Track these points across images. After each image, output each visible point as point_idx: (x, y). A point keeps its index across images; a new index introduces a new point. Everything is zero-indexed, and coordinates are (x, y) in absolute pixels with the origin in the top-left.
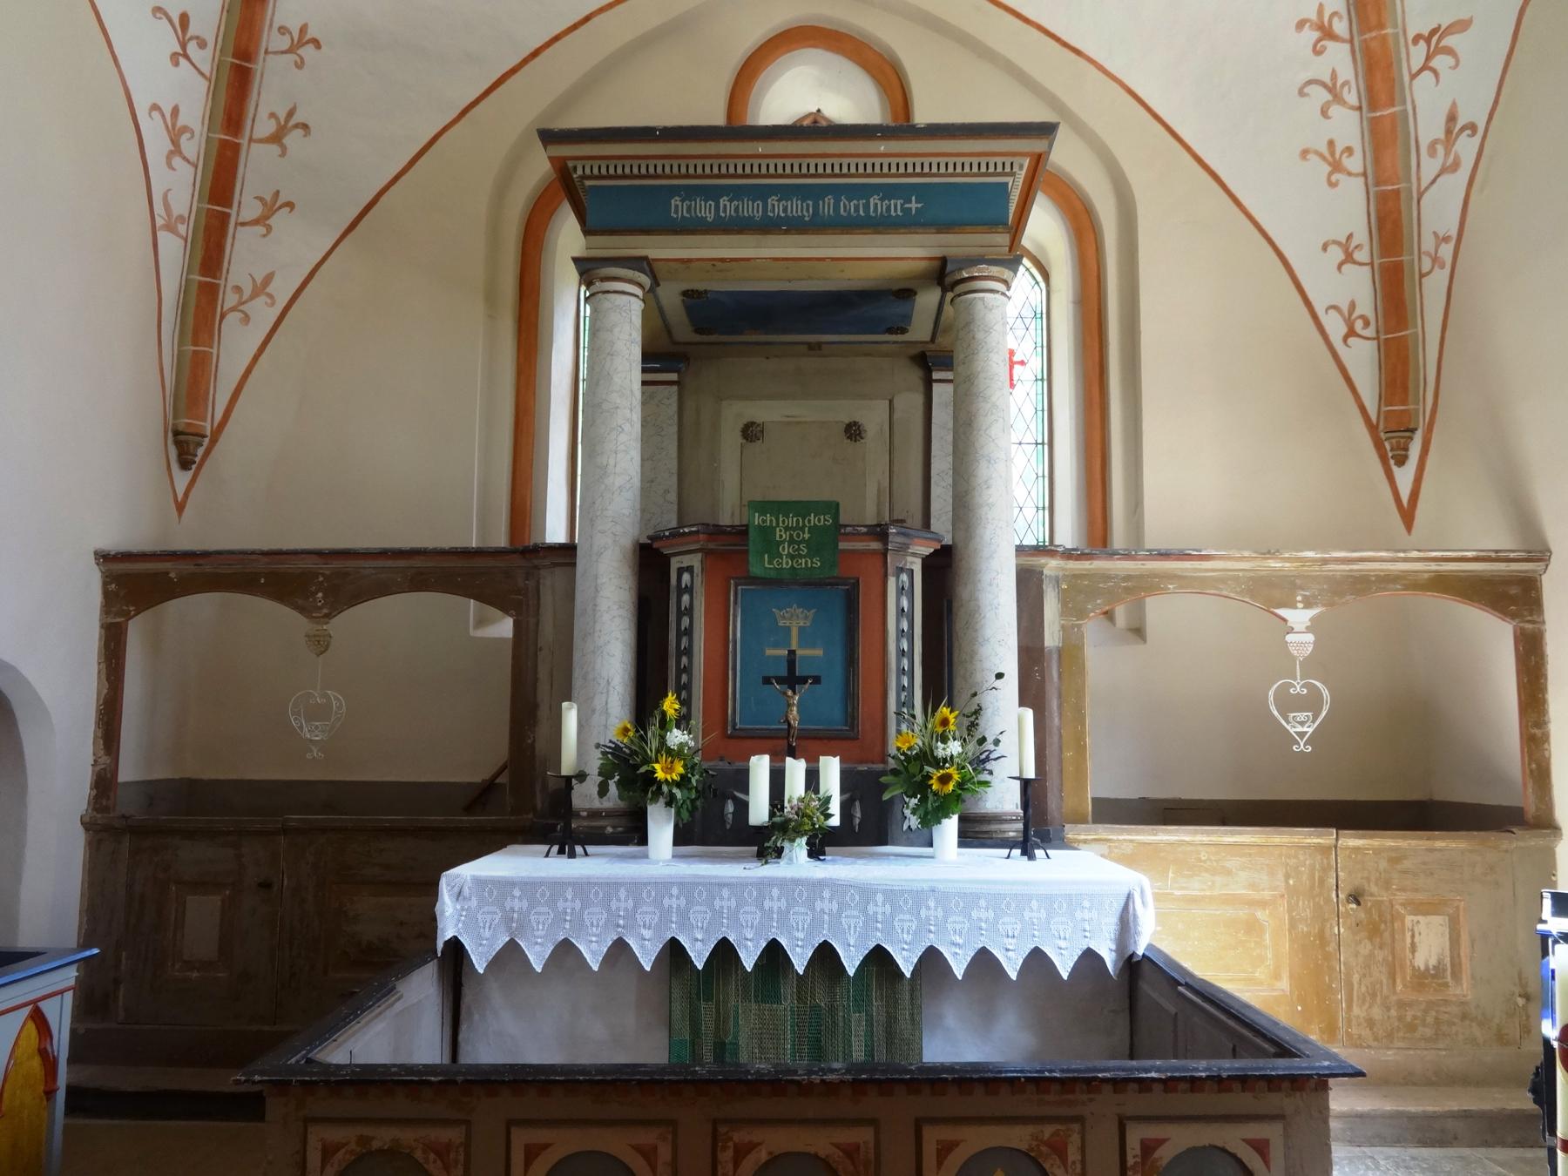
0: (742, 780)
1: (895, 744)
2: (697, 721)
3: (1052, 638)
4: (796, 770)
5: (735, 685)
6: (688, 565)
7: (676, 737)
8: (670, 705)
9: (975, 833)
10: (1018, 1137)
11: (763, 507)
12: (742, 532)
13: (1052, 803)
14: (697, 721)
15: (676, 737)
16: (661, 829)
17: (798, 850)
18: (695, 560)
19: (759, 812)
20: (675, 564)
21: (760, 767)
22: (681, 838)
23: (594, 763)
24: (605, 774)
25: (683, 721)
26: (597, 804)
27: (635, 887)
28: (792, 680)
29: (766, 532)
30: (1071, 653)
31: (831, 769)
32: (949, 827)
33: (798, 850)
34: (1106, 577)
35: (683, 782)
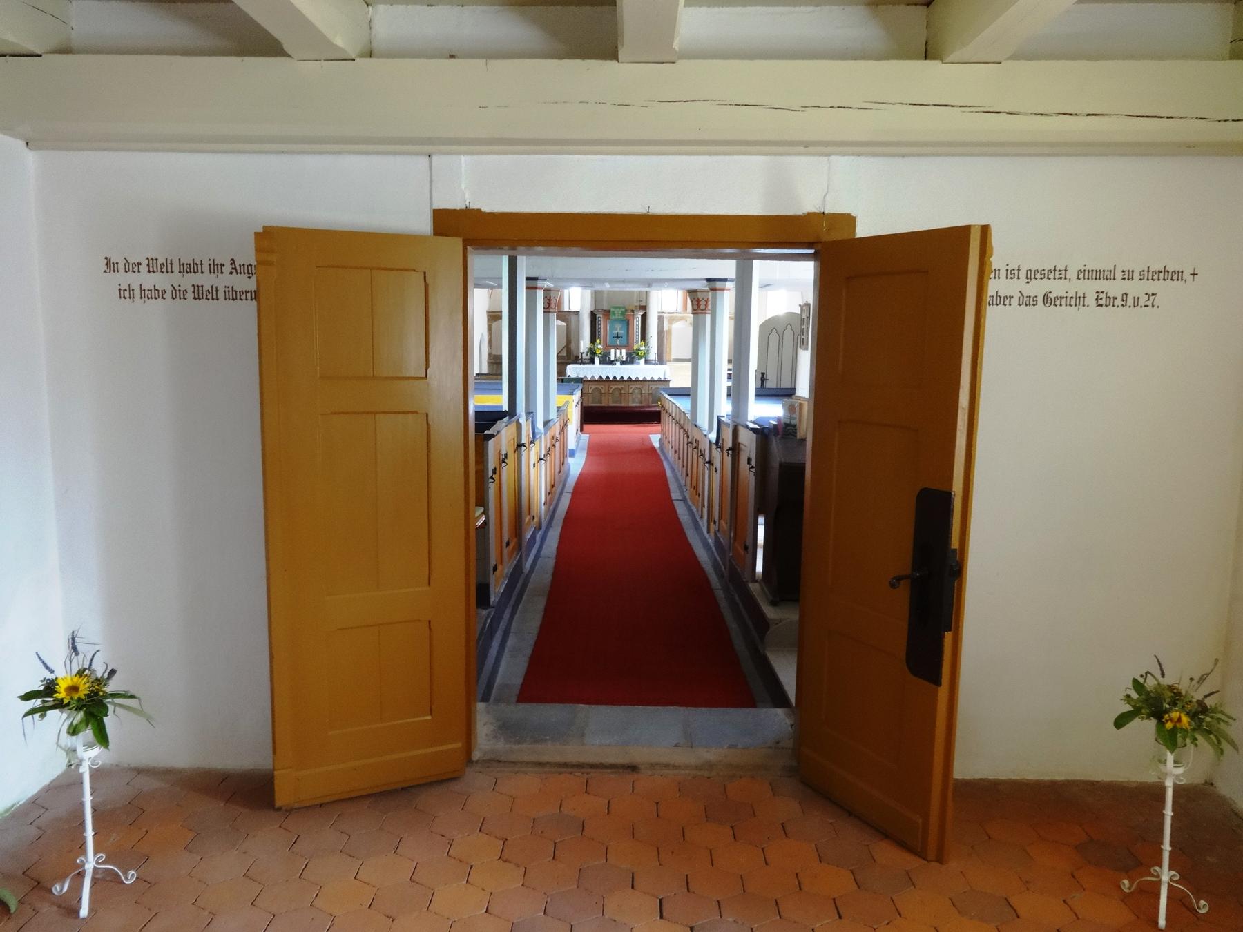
0: (609, 353)
1: (635, 348)
2: (602, 344)
3: (666, 328)
4: (618, 351)
5: (608, 337)
6: (599, 316)
7: (600, 347)
8: (598, 341)
9: (647, 362)
10: (639, 386)
11: (613, 307)
12: (609, 311)
13: (664, 358)
14: (602, 344)
15: (600, 347)
16: (597, 360)
17: (618, 364)
18: (601, 316)
19: (612, 359)
20: (597, 316)
21: (613, 351)
22: (600, 363)
23: (587, 350)
24: (588, 352)
25: (600, 344)
26: (586, 357)
27: (595, 368)
28: (618, 337)
29: (614, 312)
30: (669, 332)
31: (624, 351)
32: (643, 360)
33: (618, 364)
34: (676, 317)
35: (601, 353)
